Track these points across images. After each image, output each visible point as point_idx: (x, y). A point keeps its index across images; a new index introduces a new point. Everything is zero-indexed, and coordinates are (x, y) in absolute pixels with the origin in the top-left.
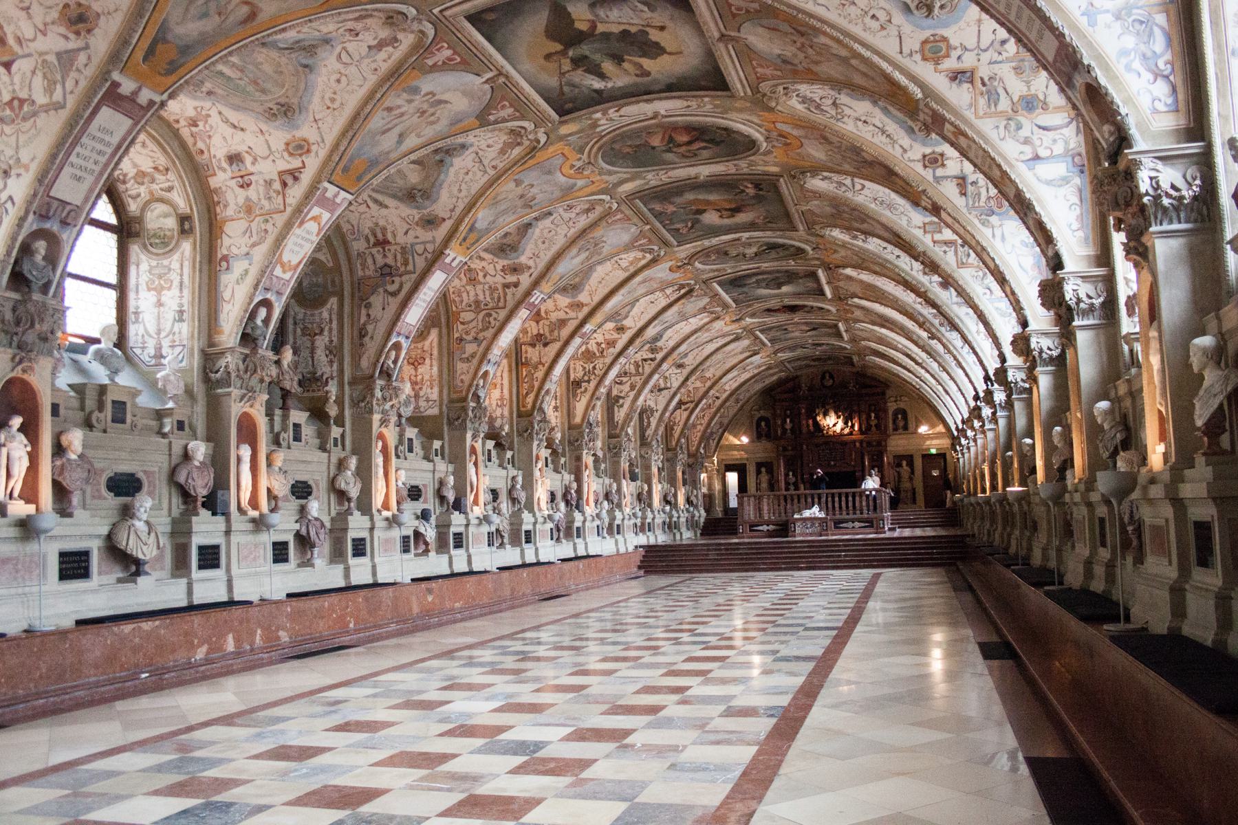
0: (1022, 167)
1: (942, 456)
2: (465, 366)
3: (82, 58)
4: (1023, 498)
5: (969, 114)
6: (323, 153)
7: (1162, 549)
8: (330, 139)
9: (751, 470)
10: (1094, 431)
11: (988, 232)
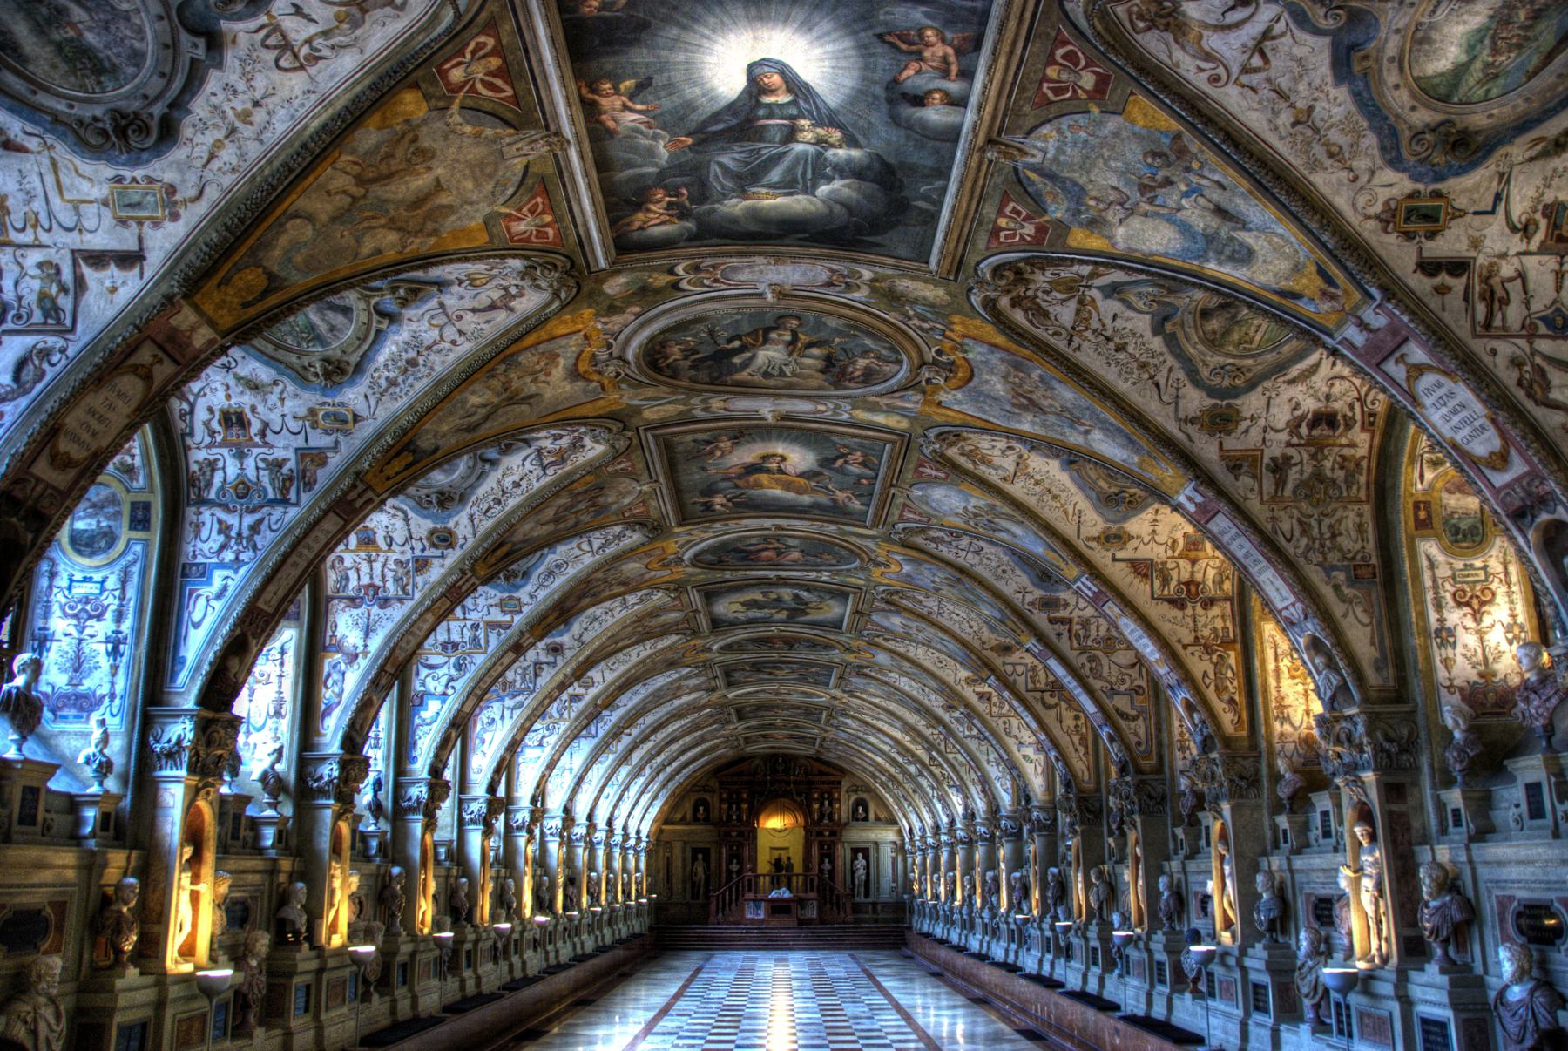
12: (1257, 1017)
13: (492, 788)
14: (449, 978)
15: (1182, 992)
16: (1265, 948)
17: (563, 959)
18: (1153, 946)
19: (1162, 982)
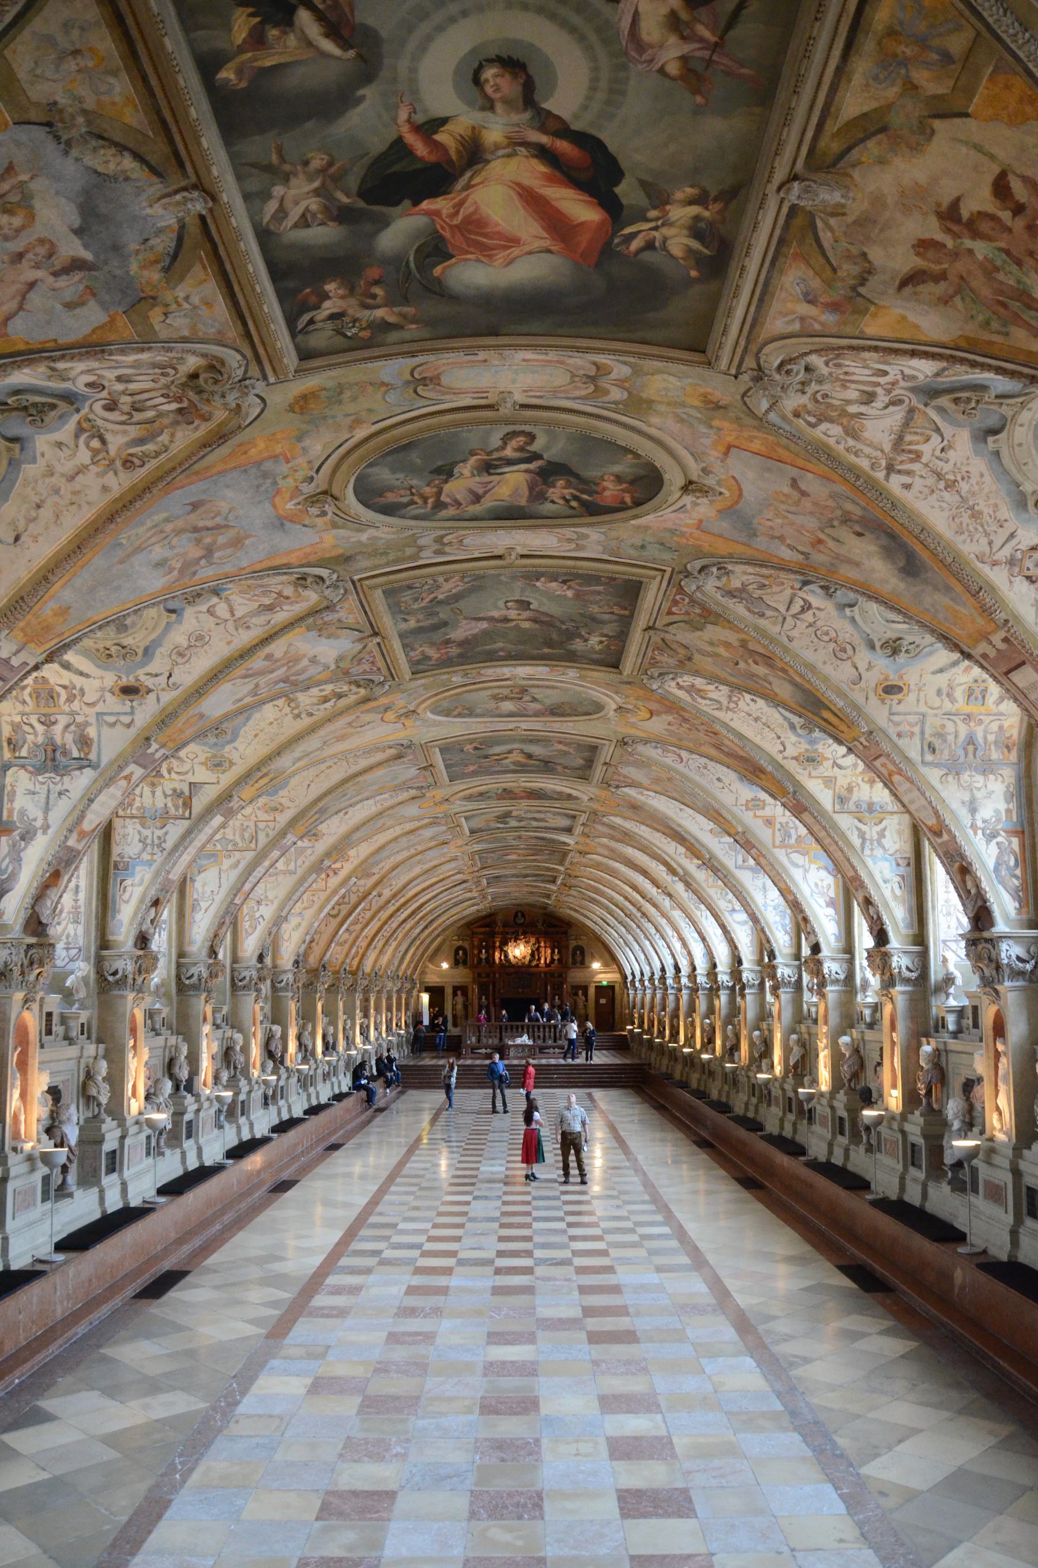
0: (727, 914)
1: (611, 988)
2: (338, 948)
3: (309, 851)
4: (710, 1061)
5: (704, 885)
6: (356, 862)
7: (777, 1105)
8: (362, 856)
9: (449, 991)
10: (752, 1044)
11: (699, 913)
12: (913, 1171)
13: (261, 958)
14: (227, 1126)
15: (857, 1144)
16: (922, 1115)
17: (324, 1100)
18: (836, 1104)
19: (842, 1133)
